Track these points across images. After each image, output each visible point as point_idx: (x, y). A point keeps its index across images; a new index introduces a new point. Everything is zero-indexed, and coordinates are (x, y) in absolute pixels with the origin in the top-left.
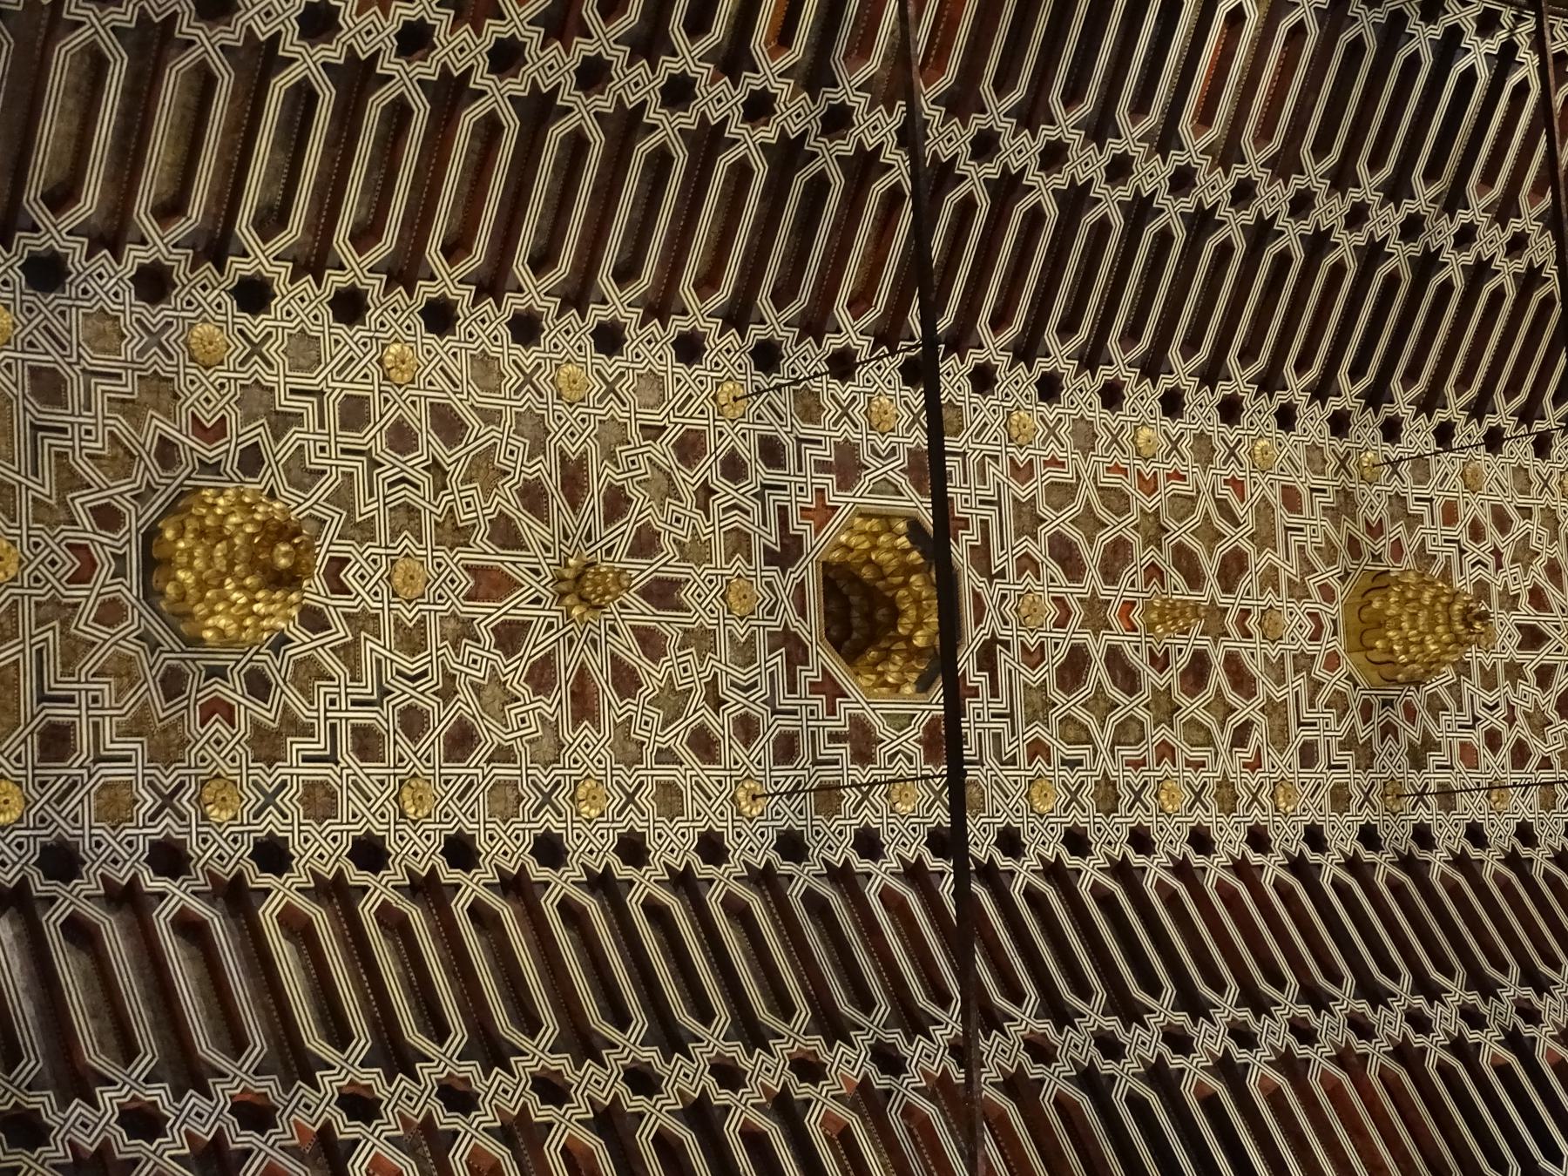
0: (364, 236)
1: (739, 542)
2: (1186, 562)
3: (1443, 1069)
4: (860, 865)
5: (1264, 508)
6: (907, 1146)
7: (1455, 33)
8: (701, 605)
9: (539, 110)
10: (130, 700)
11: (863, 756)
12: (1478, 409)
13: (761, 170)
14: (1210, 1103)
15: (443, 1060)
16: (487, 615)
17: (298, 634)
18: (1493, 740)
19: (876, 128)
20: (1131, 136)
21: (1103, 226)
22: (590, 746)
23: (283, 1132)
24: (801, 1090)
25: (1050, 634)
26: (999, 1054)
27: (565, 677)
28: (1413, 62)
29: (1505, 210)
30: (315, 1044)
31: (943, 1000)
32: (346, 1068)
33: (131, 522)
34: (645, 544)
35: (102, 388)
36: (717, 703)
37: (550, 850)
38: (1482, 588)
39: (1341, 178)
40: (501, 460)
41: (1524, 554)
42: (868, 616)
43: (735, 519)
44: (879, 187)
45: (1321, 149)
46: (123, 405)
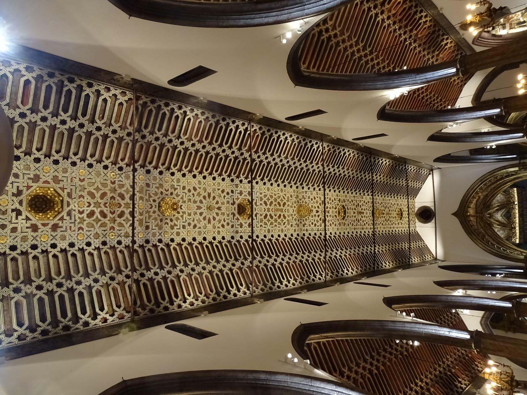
0: (186, 167)
2: (279, 203)
3: (305, 263)
4: (240, 240)
5: (288, 197)
6: (244, 274)
7: (313, 144)
8: (223, 209)
10: (156, 222)
14: (279, 268)
16: (199, 212)
17: (176, 214)
18: (312, 223)
19: (246, 155)
20: (276, 156)
21: (272, 166)
22: (210, 226)
23: (173, 275)
24: (233, 268)
26: (255, 262)
27: (207, 218)
28: (308, 147)
29: (317, 164)
30: (177, 264)
31: (249, 256)
32: (180, 266)
33: (157, 201)
34: (217, 203)
35: (154, 185)
36: (225, 221)
37: (205, 239)
39: (299, 160)
40: (201, 193)
44: (246, 161)
45: (297, 157)
46: (156, 187)
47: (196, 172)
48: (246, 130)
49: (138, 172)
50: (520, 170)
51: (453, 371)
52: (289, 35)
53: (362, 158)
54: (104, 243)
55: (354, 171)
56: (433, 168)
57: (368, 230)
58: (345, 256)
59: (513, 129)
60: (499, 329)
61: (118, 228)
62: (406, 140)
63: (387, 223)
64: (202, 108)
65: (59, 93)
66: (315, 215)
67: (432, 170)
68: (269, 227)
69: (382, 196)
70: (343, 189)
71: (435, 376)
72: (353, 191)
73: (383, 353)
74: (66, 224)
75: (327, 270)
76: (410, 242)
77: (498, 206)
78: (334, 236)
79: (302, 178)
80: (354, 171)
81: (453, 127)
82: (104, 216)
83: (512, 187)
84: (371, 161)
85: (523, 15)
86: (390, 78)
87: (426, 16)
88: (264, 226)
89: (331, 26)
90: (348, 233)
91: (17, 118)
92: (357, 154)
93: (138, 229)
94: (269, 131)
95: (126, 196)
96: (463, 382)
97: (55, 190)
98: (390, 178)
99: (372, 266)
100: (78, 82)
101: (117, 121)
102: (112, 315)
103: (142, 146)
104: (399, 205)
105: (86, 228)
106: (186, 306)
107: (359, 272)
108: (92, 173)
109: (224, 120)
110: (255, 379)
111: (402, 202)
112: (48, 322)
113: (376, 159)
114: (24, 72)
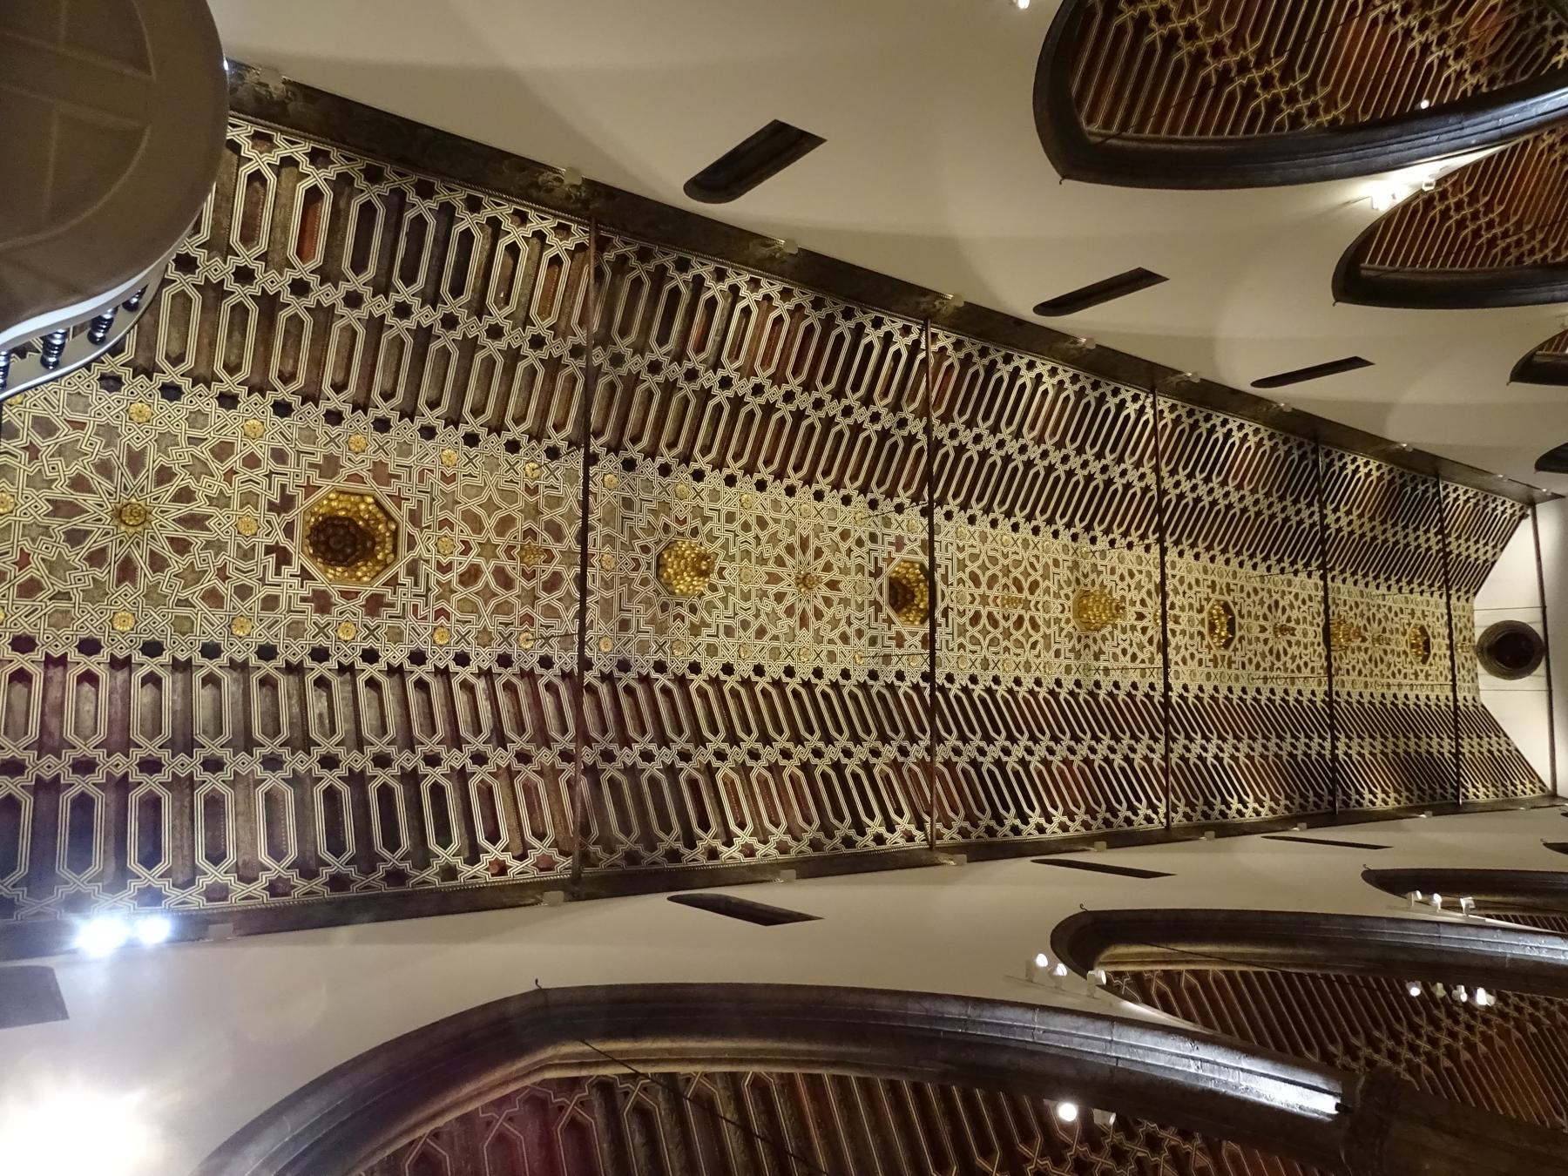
0: (737, 456)
1: (860, 568)
2: (1017, 582)
3: (1101, 767)
4: (897, 683)
5: (1046, 566)
6: (909, 783)
7: (1123, 402)
8: (846, 590)
9: (799, 415)
10: (650, 612)
11: (900, 645)
12: (1125, 534)
13: (875, 440)
14: (1016, 774)
15: (750, 742)
16: (772, 589)
17: (707, 593)
18: (1124, 652)
19: (916, 427)
20: (1006, 433)
21: (994, 465)
22: (805, 636)
24: (873, 760)
25: (967, 606)
26: (942, 752)
27: (798, 612)
28: (1108, 411)
29: (1138, 464)
30: (707, 734)
31: (924, 732)
32: (717, 742)
35: (646, 504)
36: (850, 624)
37: (790, 672)
38: (1123, 598)
39: (1080, 451)
40: (780, 536)
41: (1139, 587)
43: (859, 560)
44: (916, 447)
45: (1073, 440)
46: (652, 511)
47: (764, 473)
48: (914, 348)
49: (601, 464)
53: (1288, 453)
54: (505, 661)
55: (1260, 495)
56: (1536, 494)
57: (1312, 687)
61: (543, 621)
63: (1376, 671)
64: (782, 275)
65: (393, 227)
66: (1133, 628)
67: (1532, 503)
68: (985, 652)
69: (1355, 583)
72: (1258, 559)
74: (403, 597)
76: (1458, 737)
78: (1197, 697)
79: (1091, 508)
80: (1260, 495)
82: (506, 582)
86: (1371, 136)
88: (969, 647)
90: (1244, 690)
91: (286, 296)
92: (1271, 437)
93: (599, 628)
95: (566, 531)
97: (377, 503)
98: (1383, 522)
99: (1327, 797)
100: (443, 196)
101: (544, 312)
102: (522, 857)
103: (612, 387)
104: (1418, 614)
105: (456, 615)
106: (731, 855)
108: (477, 461)
109: (848, 315)
111: (1428, 605)
112: (347, 856)
113: (1335, 456)
114: (305, 166)
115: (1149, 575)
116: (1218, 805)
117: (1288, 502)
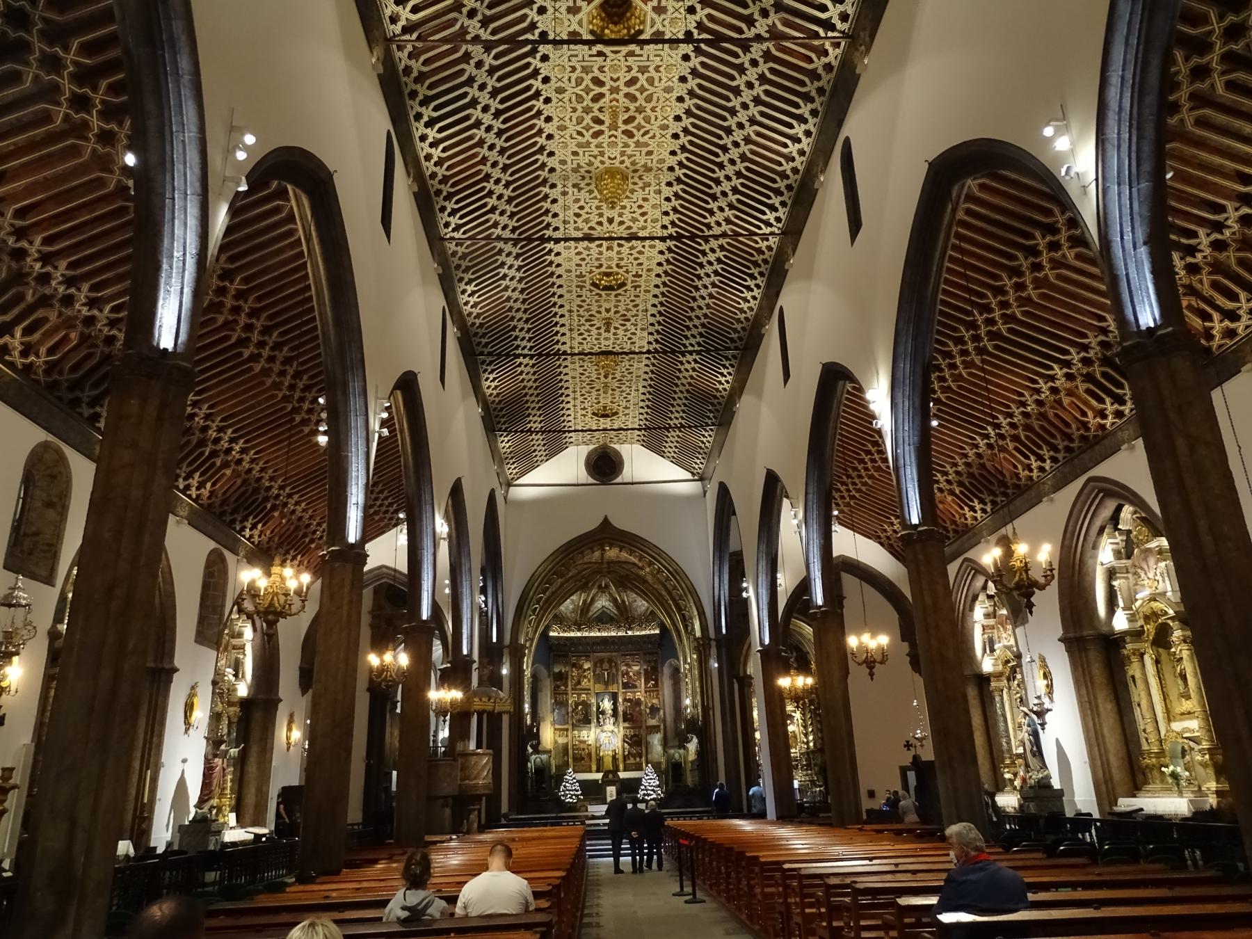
2: (630, 120)
3: (484, 188)
5: (647, 145)
7: (776, 210)
14: (467, 118)
18: (581, 208)
20: (754, 111)
21: (729, 100)
25: (608, 75)
26: (477, 51)
28: (769, 198)
29: (728, 221)
31: (493, 33)
38: (624, 207)
39: (739, 174)
42: (615, 14)
44: (744, 26)
45: (748, 169)
48: (828, 25)
50: (696, 639)
51: (276, 514)
52: (1062, 144)
53: (735, 330)
55: (705, 311)
57: (569, 342)
58: (506, 288)
59: (780, 628)
60: (374, 600)
62: (773, 422)
66: (601, 215)
67: (701, 479)
70: (664, 284)
71: (259, 479)
72: (659, 308)
73: (291, 371)
75: (469, 242)
76: (543, 432)
77: (623, 601)
79: (695, 184)
81: (791, 519)
83: (662, 627)
84: (729, 349)
85: (1009, 648)
87: (1041, 469)
88: (574, 76)
89: (1064, 256)
90: (561, 296)
94: (821, 91)
96: (256, 532)
98: (688, 391)
99: (486, 351)
107: (470, 320)
110: (172, 41)
111: (633, 417)
113: (733, 362)
115: (644, 228)
116: (467, 277)
117: (701, 330)
